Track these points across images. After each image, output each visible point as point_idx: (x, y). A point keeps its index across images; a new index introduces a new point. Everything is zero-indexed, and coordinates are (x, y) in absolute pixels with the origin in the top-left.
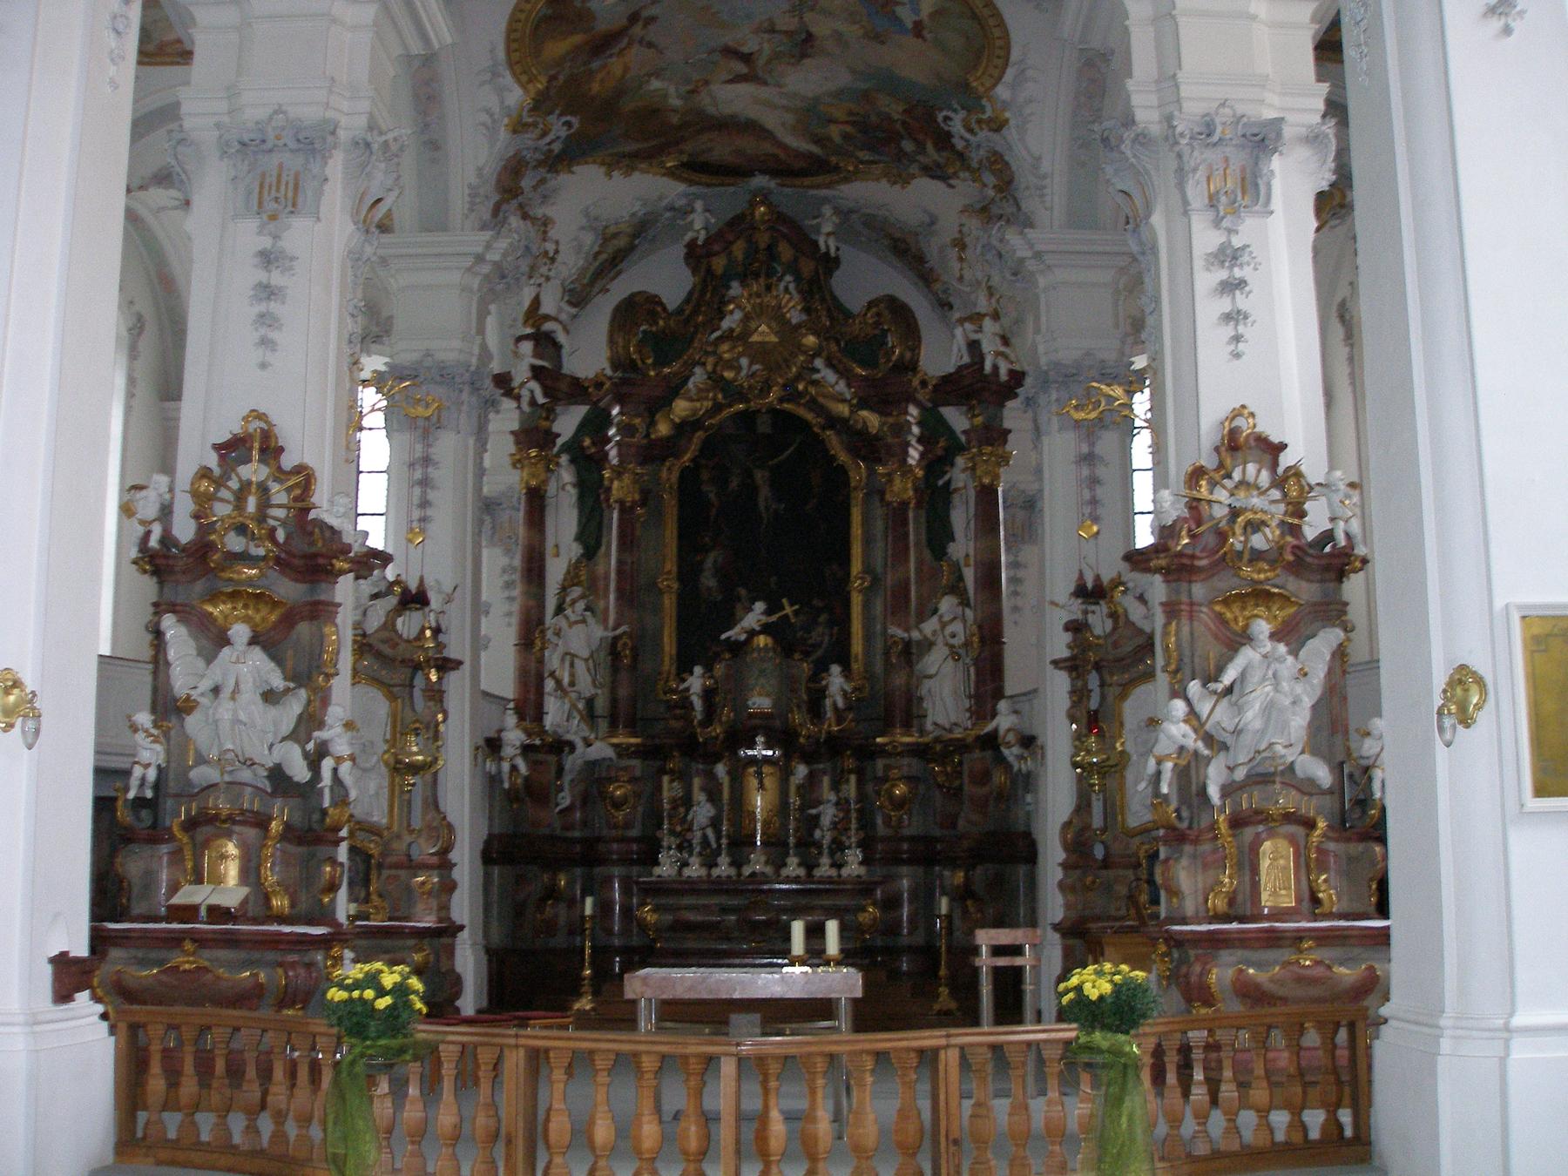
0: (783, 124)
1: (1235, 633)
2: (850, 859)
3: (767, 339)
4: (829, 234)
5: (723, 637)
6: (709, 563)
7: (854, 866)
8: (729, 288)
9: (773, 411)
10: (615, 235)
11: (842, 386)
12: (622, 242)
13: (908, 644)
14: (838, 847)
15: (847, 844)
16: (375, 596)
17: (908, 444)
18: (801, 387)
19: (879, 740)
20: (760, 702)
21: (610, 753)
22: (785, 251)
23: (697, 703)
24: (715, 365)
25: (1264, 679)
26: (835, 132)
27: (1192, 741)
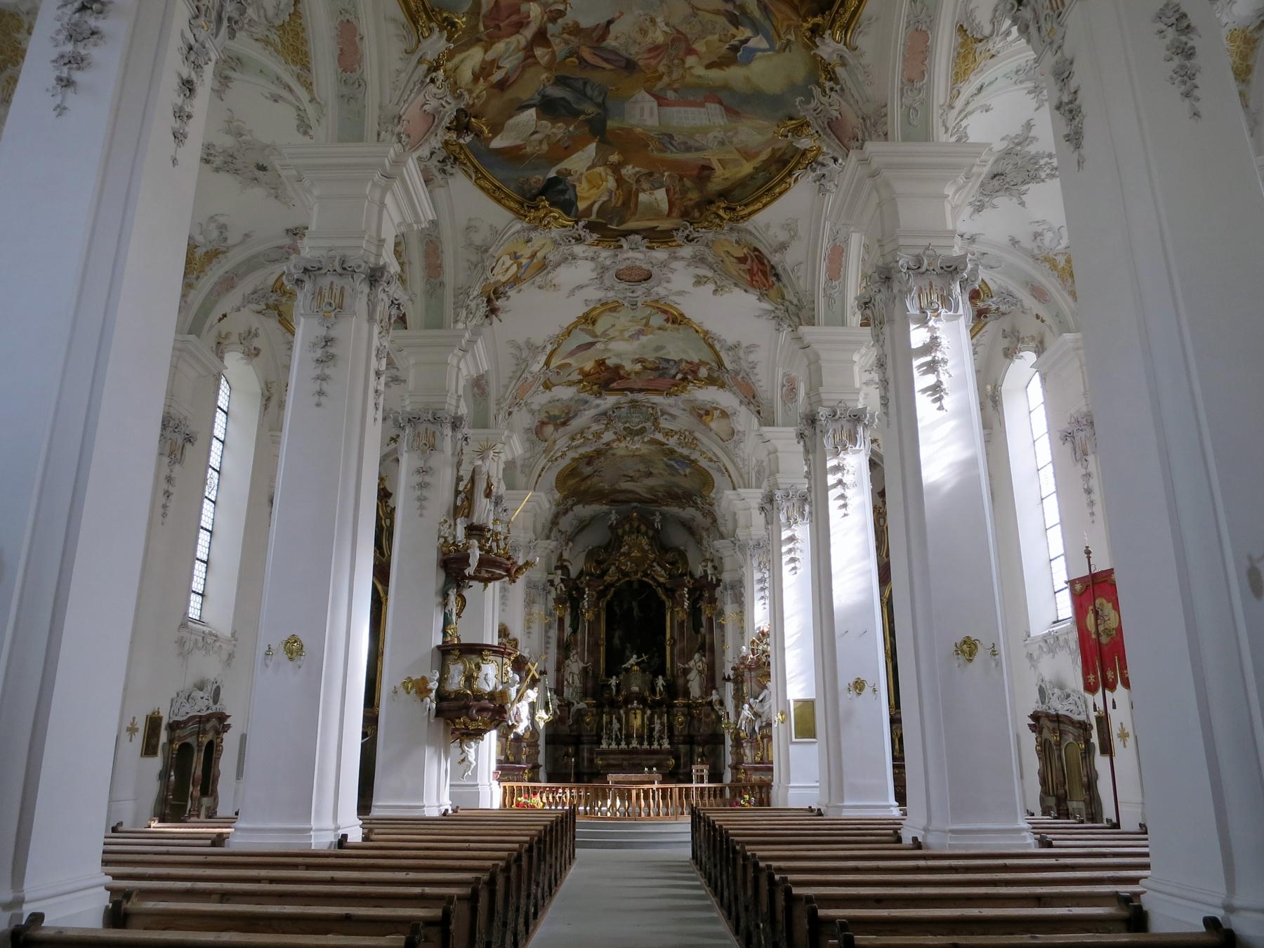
6: (617, 635)
7: (666, 745)
11: (663, 572)
12: (587, 522)
13: (684, 669)
14: (661, 738)
17: (684, 601)
20: (635, 689)
21: (585, 706)
22: (643, 528)
23: (614, 689)
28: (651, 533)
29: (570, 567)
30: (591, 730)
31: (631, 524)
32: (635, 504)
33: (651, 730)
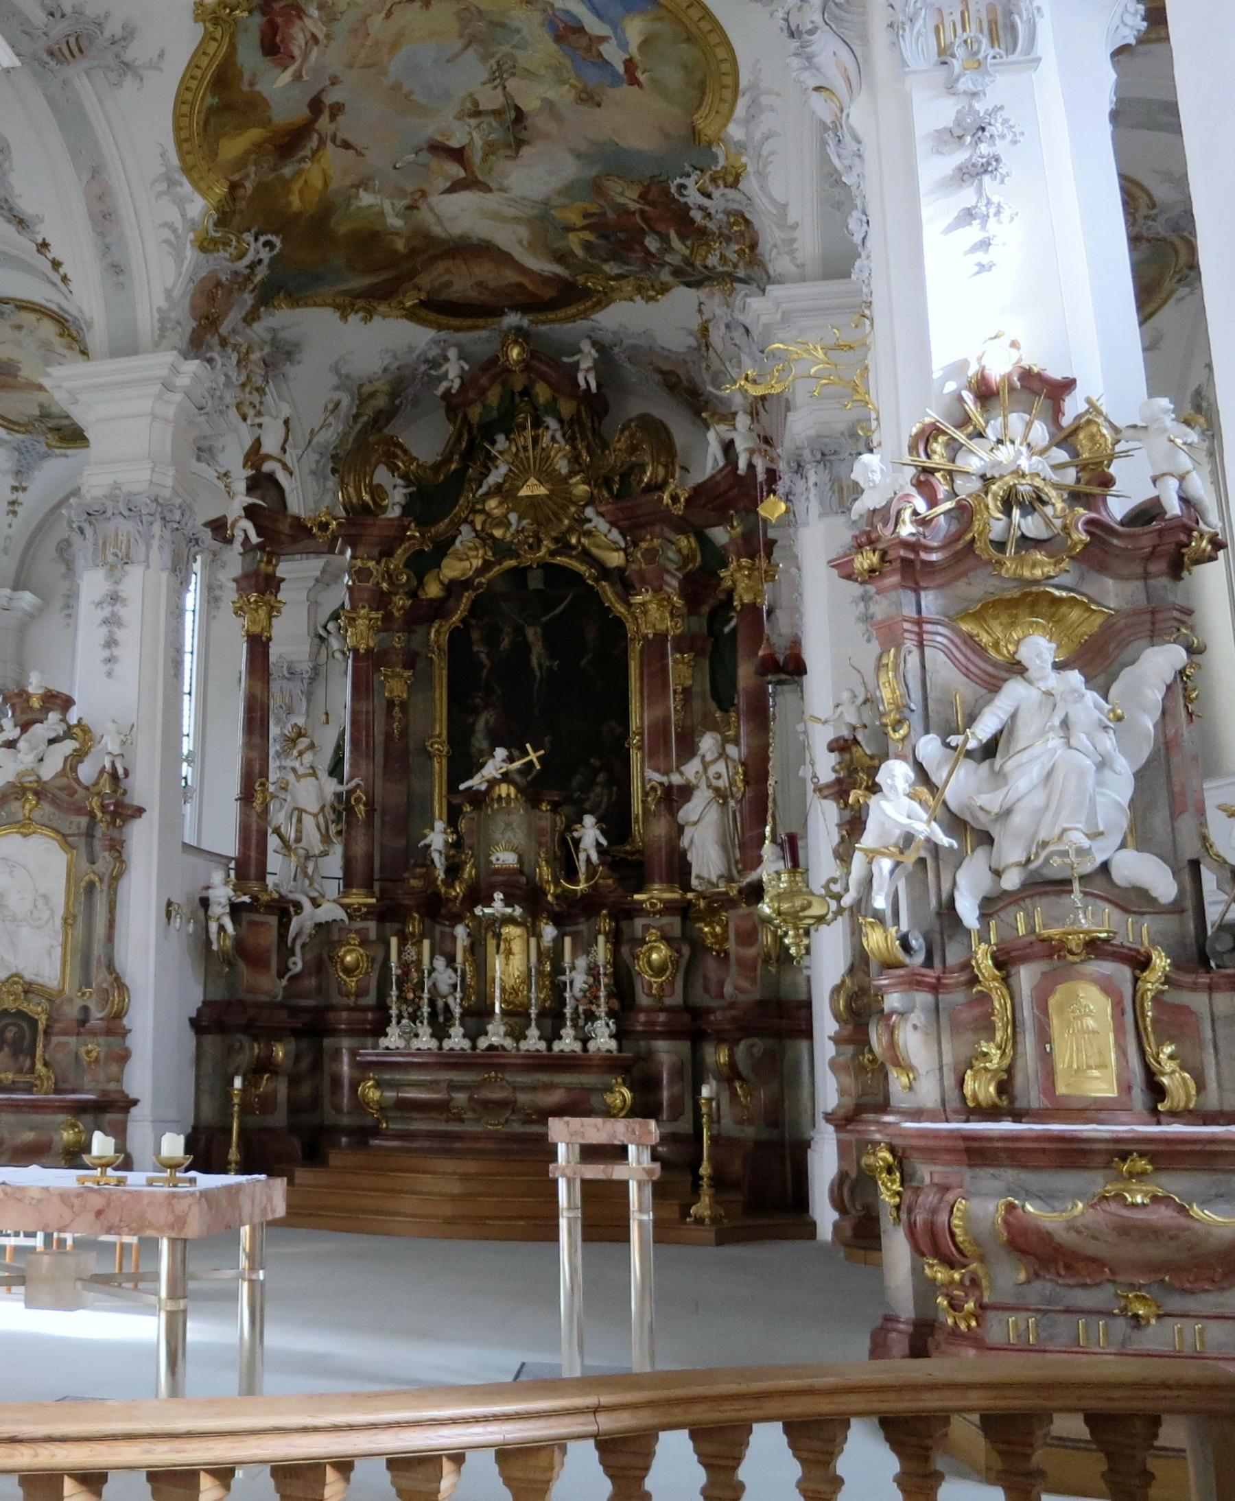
0: (520, 242)
1: (995, 664)
2: (599, 1032)
3: (536, 492)
4: (588, 370)
5: (462, 787)
6: (481, 724)
7: (603, 1040)
8: (493, 443)
9: (545, 566)
10: (373, 395)
13: (668, 789)
15: (597, 1014)
16: (52, 741)
18: (574, 541)
19: (636, 897)
20: (505, 858)
21: (340, 914)
22: (542, 392)
24: (483, 524)
25: (1042, 733)
26: (574, 242)
27: (926, 828)
28: (567, 408)
29: (281, 477)
30: (361, 992)
31: (504, 384)
32: (512, 319)
33: (558, 990)
